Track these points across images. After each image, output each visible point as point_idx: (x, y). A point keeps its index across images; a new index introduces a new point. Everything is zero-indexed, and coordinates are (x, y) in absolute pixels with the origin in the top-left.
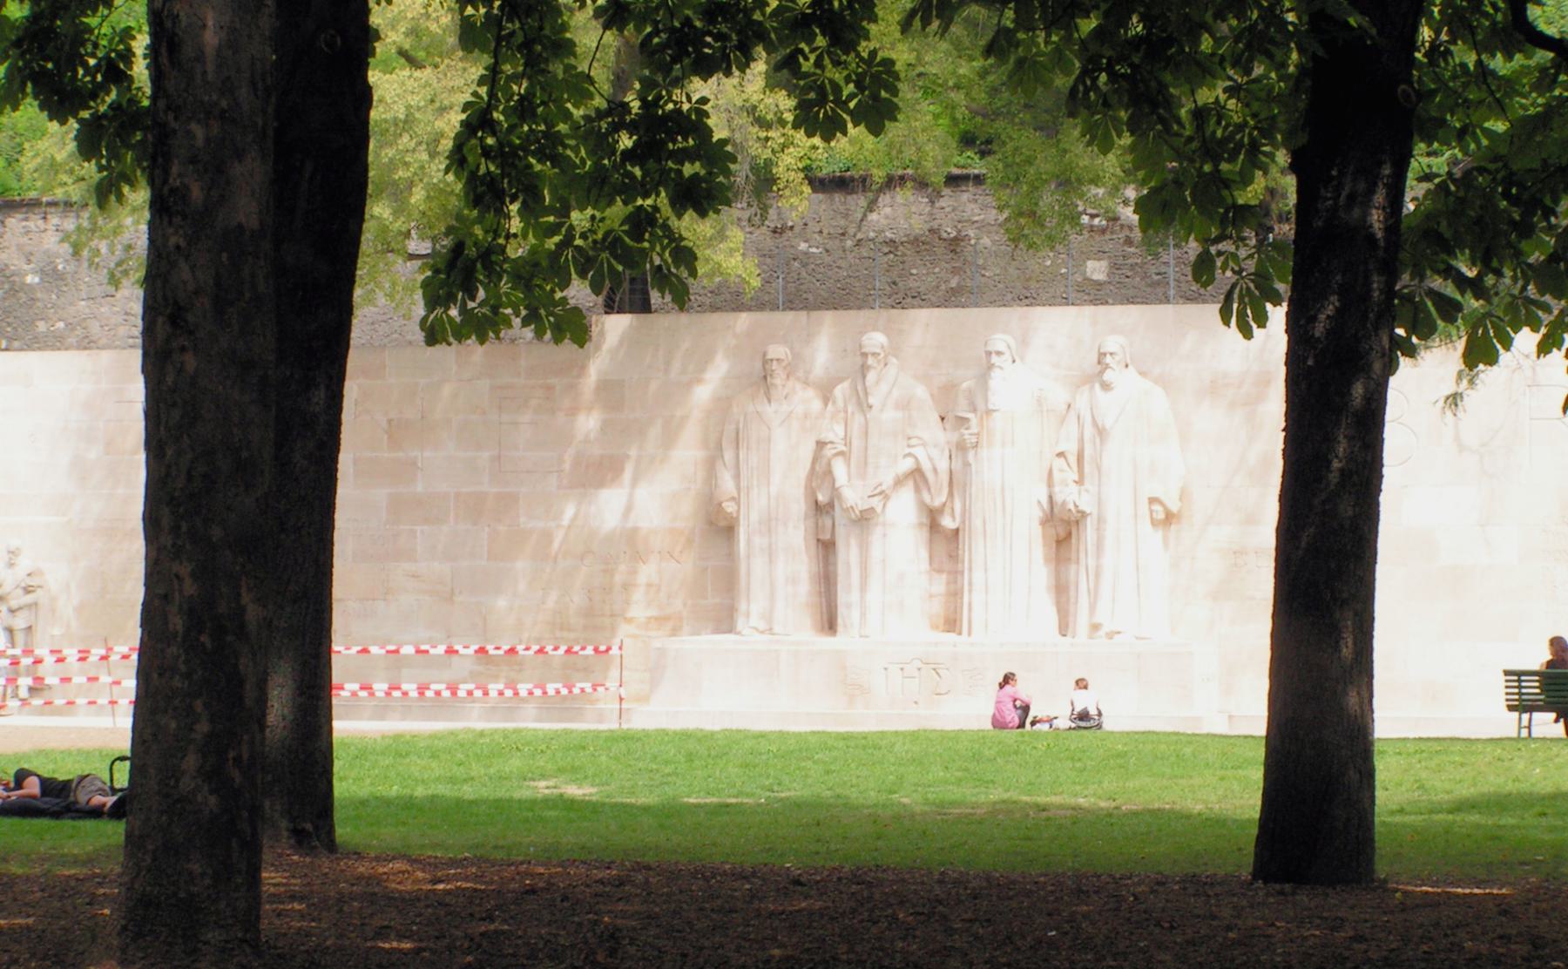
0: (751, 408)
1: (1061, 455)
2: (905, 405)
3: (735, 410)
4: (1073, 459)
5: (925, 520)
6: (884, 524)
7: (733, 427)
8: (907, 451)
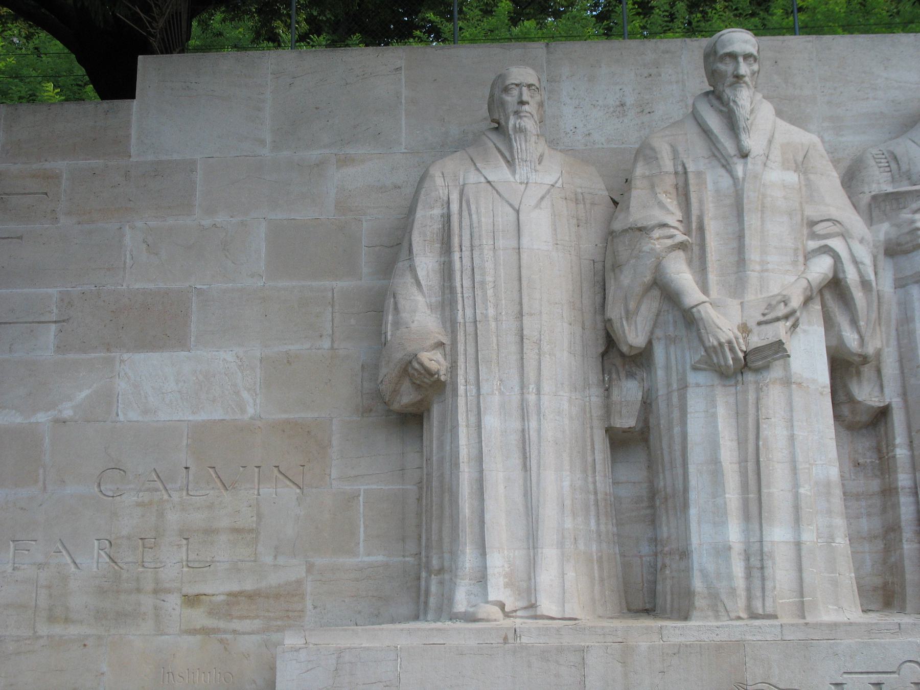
0: (473, 177)
2: (802, 165)
3: (439, 181)
6: (787, 382)
7: (437, 211)
8: (812, 245)
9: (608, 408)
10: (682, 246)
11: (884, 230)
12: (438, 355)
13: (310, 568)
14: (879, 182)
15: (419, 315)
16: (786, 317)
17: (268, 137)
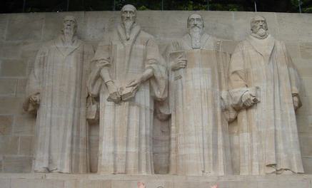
1: (235, 72)
4: (243, 75)
5: (152, 108)
7: (42, 56)
9: (87, 114)
10: (107, 65)
11: (172, 64)
12: (37, 97)
13: (4, 158)
14: (172, 50)
15: (34, 85)
16: (134, 86)
17: (5, 37)
